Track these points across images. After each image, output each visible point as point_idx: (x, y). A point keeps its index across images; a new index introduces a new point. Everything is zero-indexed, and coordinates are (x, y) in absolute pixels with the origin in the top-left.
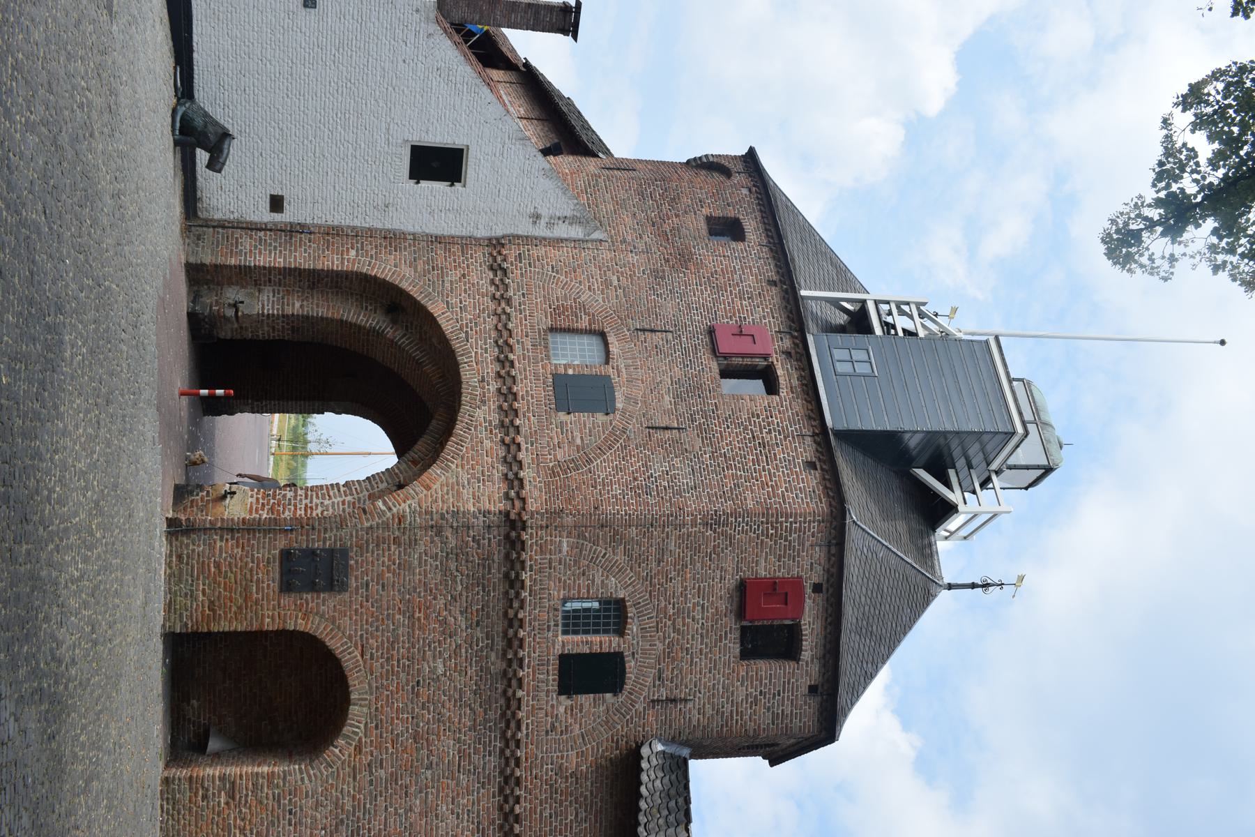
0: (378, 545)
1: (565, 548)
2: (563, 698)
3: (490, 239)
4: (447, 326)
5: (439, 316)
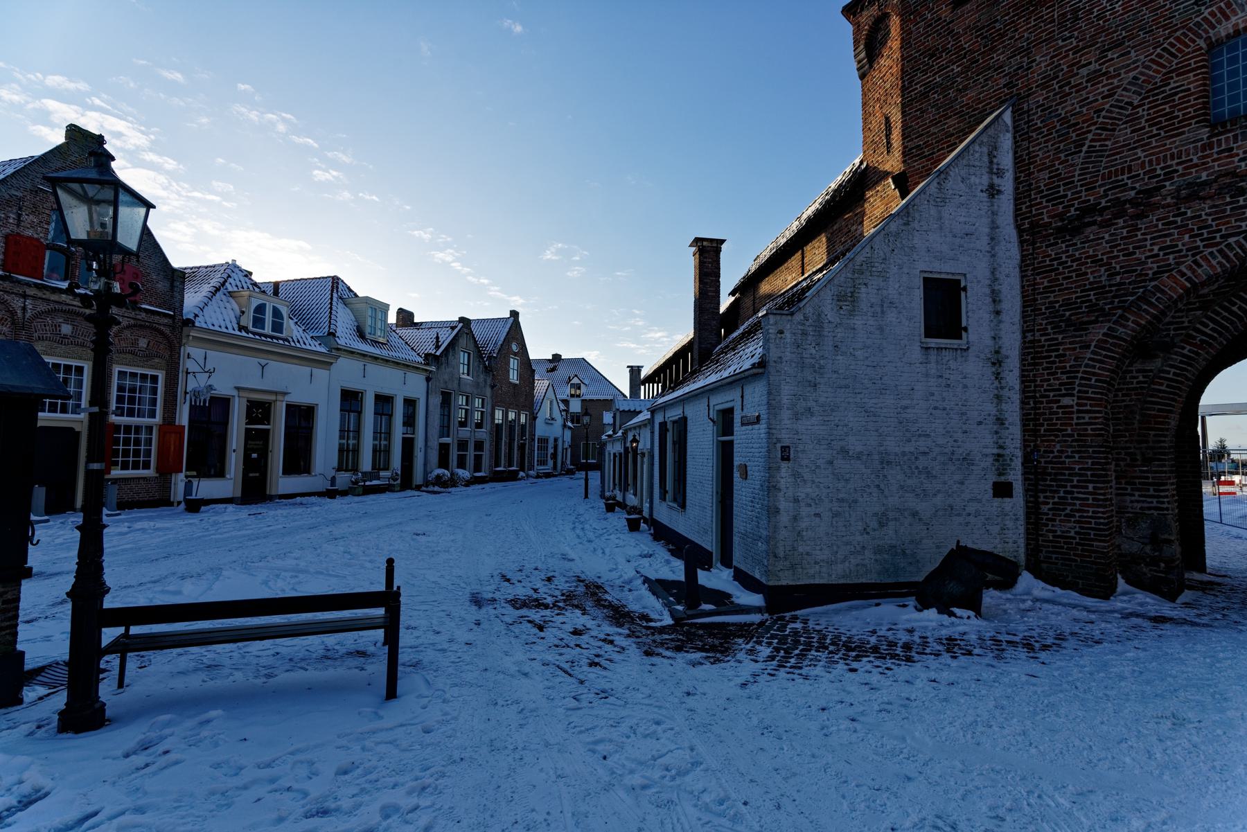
5: (1189, 279)
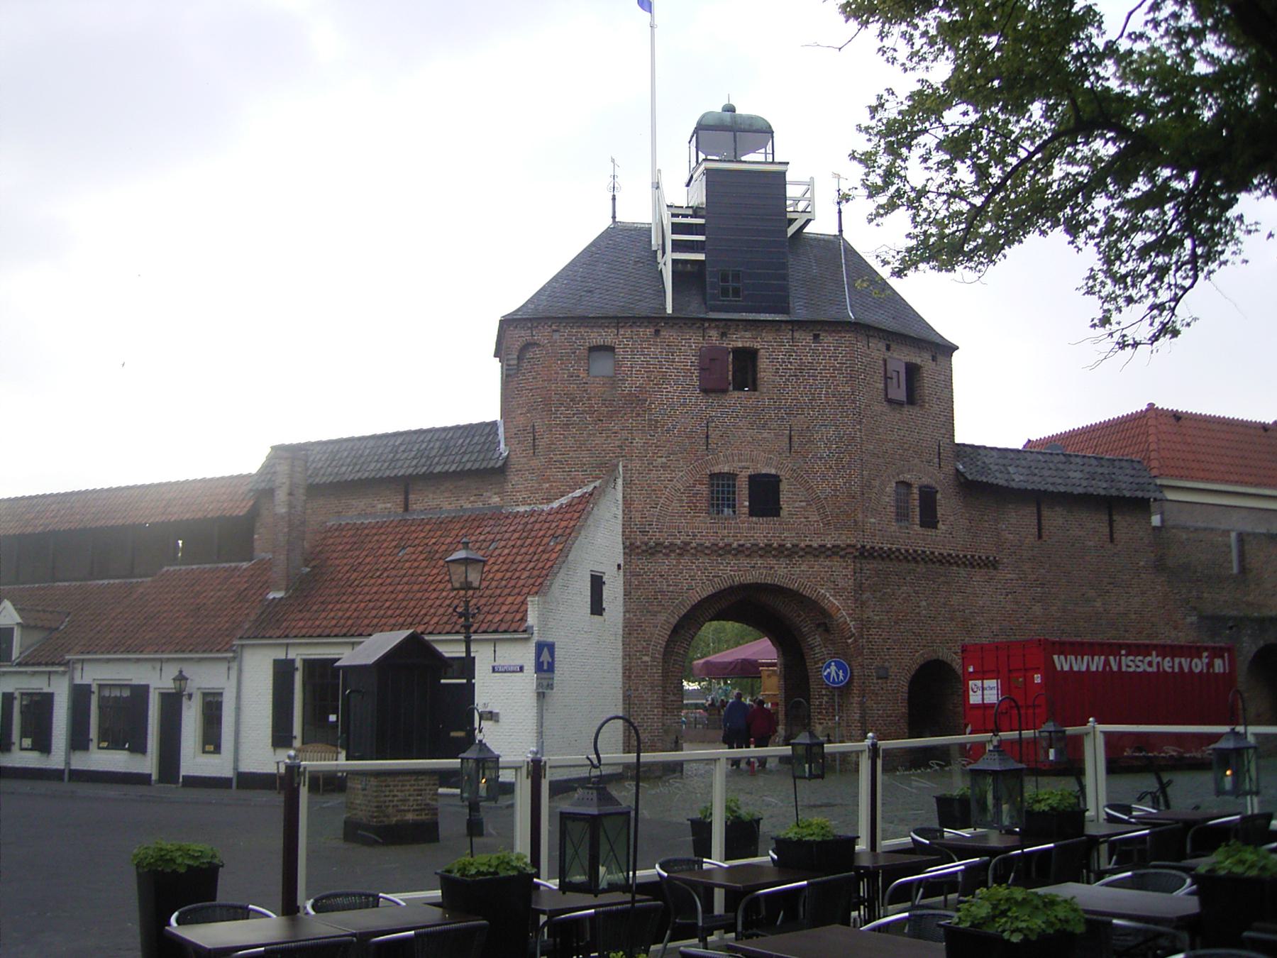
0: (870, 642)
1: (873, 520)
2: (940, 525)
3: (624, 553)
4: (710, 591)
